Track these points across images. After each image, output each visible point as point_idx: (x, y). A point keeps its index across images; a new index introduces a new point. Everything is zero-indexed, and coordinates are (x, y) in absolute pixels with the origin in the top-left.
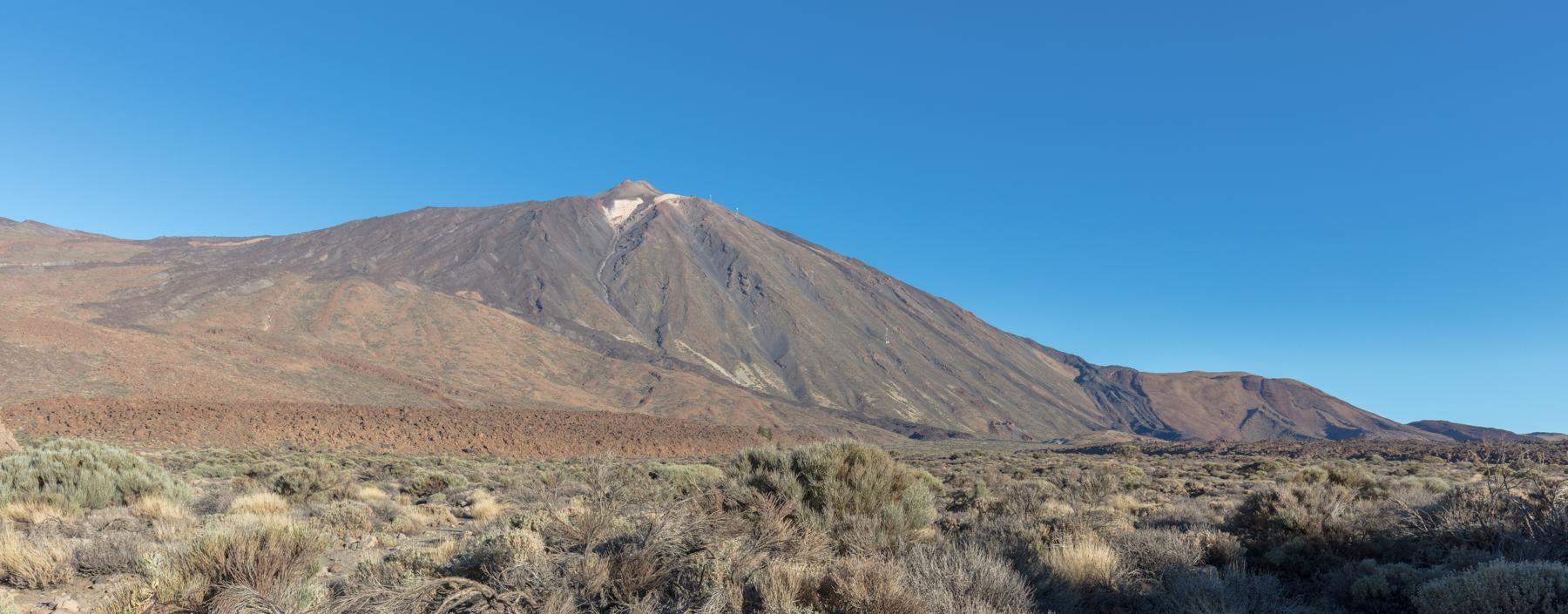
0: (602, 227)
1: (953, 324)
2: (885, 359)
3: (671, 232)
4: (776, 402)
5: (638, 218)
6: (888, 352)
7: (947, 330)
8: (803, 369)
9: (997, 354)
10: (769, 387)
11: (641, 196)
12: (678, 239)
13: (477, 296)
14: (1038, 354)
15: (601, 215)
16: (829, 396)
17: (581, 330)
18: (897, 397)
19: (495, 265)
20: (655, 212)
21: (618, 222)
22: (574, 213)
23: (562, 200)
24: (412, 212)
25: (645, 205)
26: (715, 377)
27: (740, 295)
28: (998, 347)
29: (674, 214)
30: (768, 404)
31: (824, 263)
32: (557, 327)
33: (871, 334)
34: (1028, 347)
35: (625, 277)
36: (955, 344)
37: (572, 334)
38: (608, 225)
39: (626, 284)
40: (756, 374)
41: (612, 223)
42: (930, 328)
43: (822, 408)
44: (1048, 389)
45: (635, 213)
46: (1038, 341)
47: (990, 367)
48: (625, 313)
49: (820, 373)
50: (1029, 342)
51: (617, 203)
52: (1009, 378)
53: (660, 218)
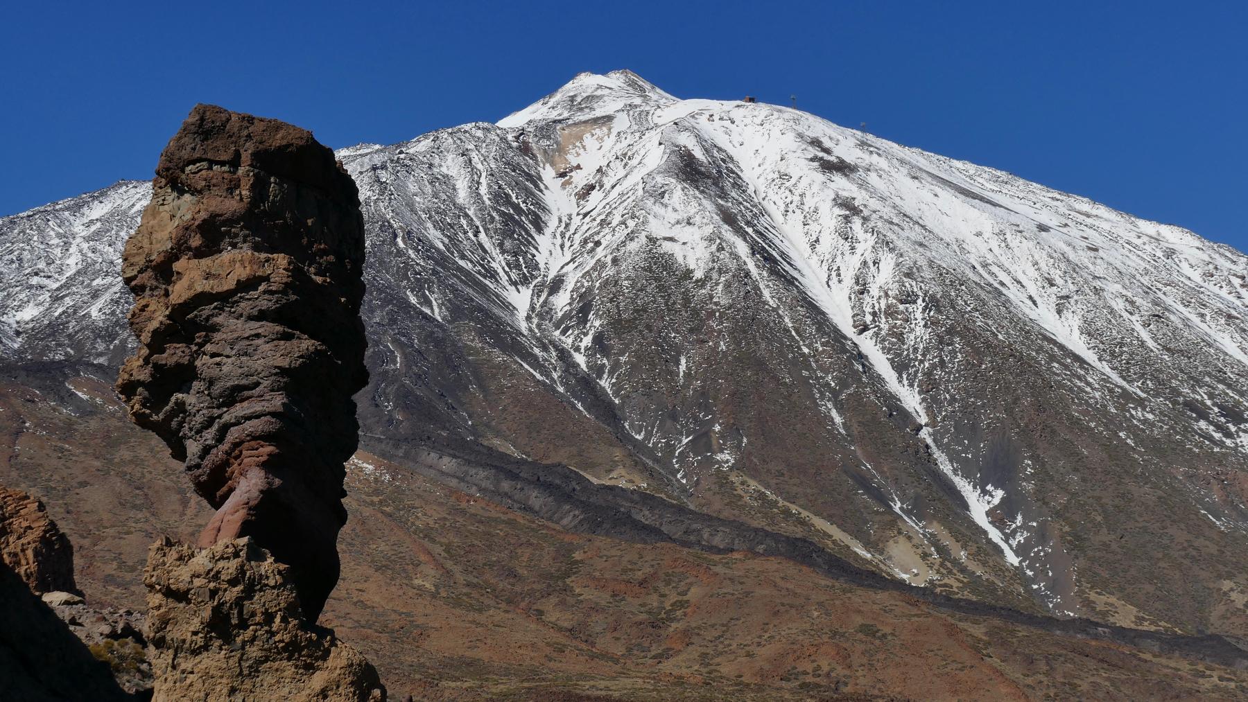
4: (997, 622)
10: (974, 583)
16: (1129, 599)
17: (503, 466)
26: (841, 567)
30: (979, 631)
32: (447, 463)
43: (1120, 633)
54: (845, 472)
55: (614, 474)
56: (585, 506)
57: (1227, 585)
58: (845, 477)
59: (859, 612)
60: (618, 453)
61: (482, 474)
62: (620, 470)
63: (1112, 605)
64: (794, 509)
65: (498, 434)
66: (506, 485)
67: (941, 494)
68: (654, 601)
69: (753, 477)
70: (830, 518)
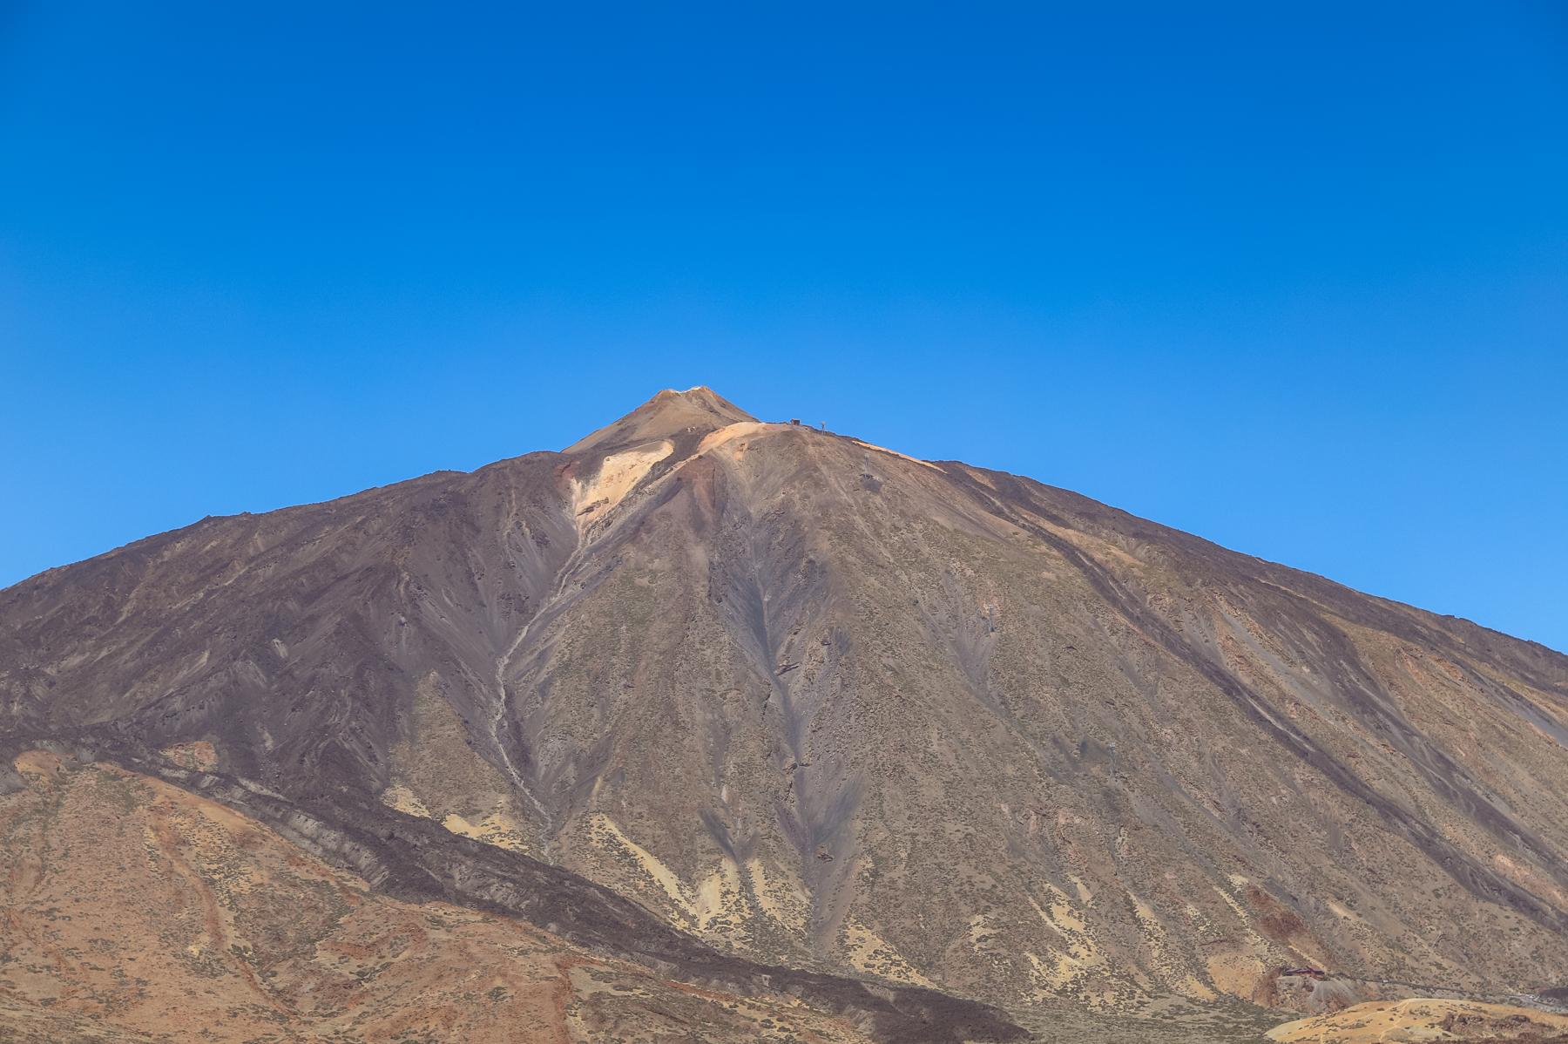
3: (689, 534)
7: (1328, 720)
15: (562, 499)
18: (1062, 919)
23: (483, 473)
24: (175, 536)
25: (669, 462)
28: (1462, 753)
31: (1056, 570)
32: (310, 826)
35: (553, 662)
36: (1321, 760)
37: (331, 838)
38: (568, 527)
39: (543, 690)
40: (746, 885)
44: (1550, 861)
45: (639, 488)
51: (611, 464)
52: (1429, 843)
54: (701, 813)
55: (488, 821)
58: (698, 818)
59: (504, 975)
60: (503, 799)
61: (333, 835)
62: (496, 818)
63: (862, 939)
64: (633, 848)
65: (406, 781)
66: (347, 846)
67: (782, 834)
68: (371, 962)
69: (613, 819)
70: (662, 858)
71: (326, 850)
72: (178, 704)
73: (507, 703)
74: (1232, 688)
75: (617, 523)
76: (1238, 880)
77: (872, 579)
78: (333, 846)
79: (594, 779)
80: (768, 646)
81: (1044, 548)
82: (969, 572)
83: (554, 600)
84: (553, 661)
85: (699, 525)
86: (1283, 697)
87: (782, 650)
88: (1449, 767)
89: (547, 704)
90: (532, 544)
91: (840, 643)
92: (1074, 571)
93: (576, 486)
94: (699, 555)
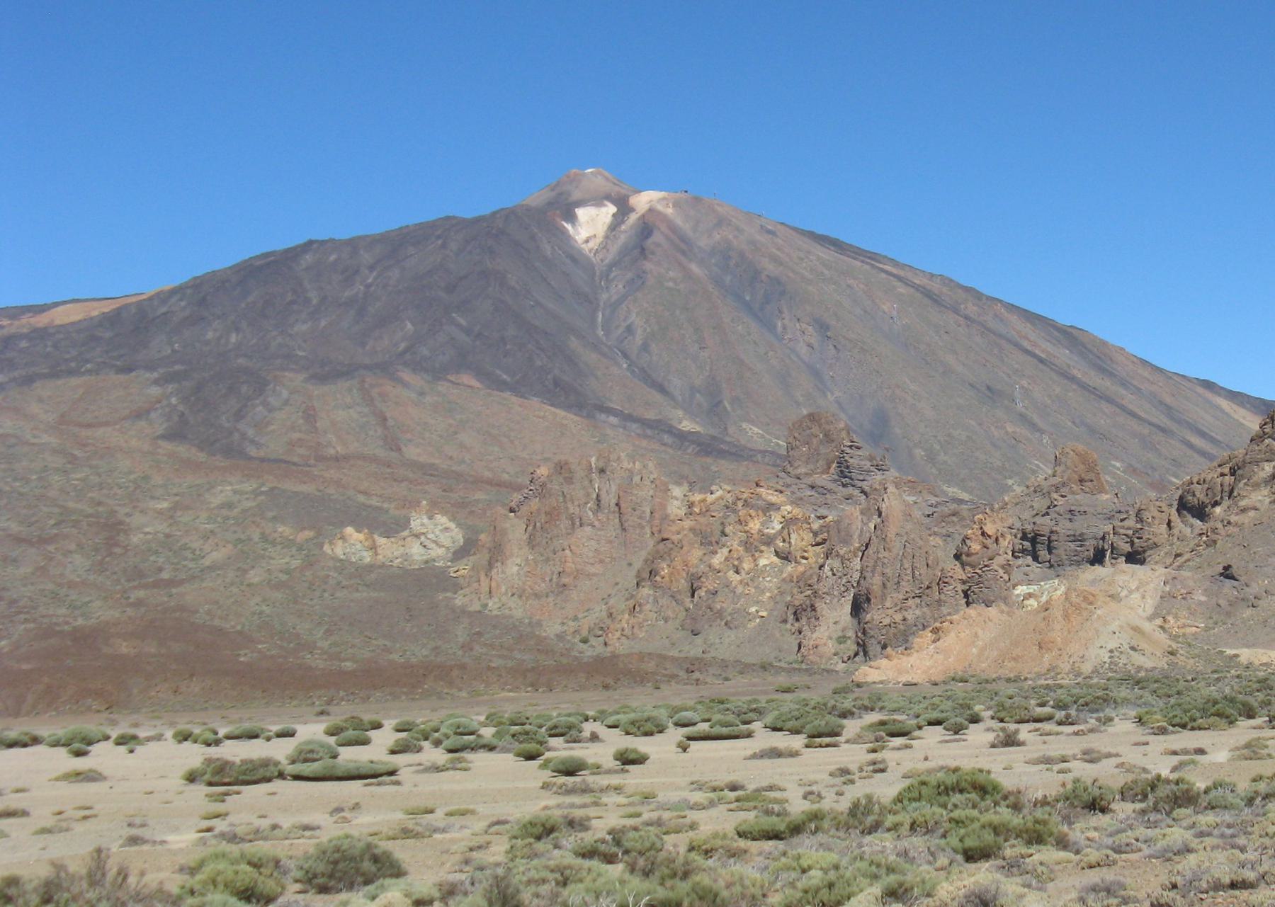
0: (575, 256)
1: (1102, 370)
2: (1022, 431)
5: (623, 238)
6: (1023, 418)
7: (1095, 380)
8: (919, 452)
9: (1169, 410)
11: (608, 197)
12: (694, 268)
13: (467, 379)
14: (1224, 404)
15: (564, 232)
16: (964, 489)
19: (468, 331)
20: (646, 228)
21: (591, 245)
22: (533, 237)
27: (803, 350)
28: (1169, 400)
29: (673, 228)
31: (902, 289)
33: (992, 394)
34: (1208, 395)
36: (1110, 400)
38: (580, 251)
39: (645, 347)
41: (586, 248)
42: (1072, 379)
46: (1221, 383)
47: (1163, 430)
48: (662, 390)
49: (942, 457)
50: (1208, 385)
51: (581, 213)
53: (657, 237)
56: (699, 445)
57: (1010, 482)
61: (634, 426)
66: (649, 432)
71: (639, 435)
72: (425, 352)
73: (625, 356)
74: (1041, 361)
75: (614, 249)
76: (1118, 465)
77: (810, 288)
78: (638, 431)
79: (720, 402)
80: (771, 328)
81: (883, 275)
82: (862, 286)
83: (604, 296)
84: (639, 331)
85: (684, 253)
86: (1069, 366)
87: (779, 329)
88: (1169, 408)
89: (654, 358)
90: (568, 261)
91: (823, 327)
92: (912, 290)
93: (569, 227)
94: (694, 268)
